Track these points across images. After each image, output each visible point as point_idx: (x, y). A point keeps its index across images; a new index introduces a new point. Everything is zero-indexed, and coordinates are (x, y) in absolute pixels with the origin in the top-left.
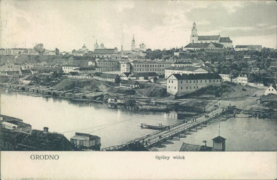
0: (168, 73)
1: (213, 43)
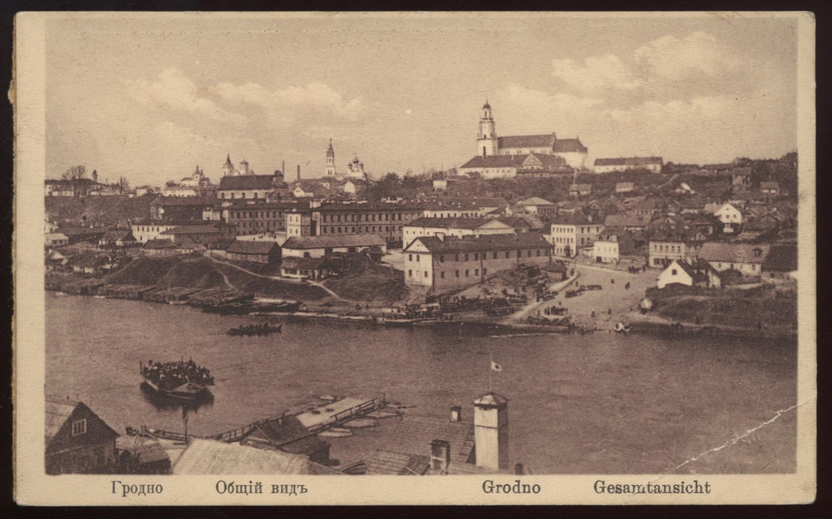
0: (410, 234)
1: (537, 155)
